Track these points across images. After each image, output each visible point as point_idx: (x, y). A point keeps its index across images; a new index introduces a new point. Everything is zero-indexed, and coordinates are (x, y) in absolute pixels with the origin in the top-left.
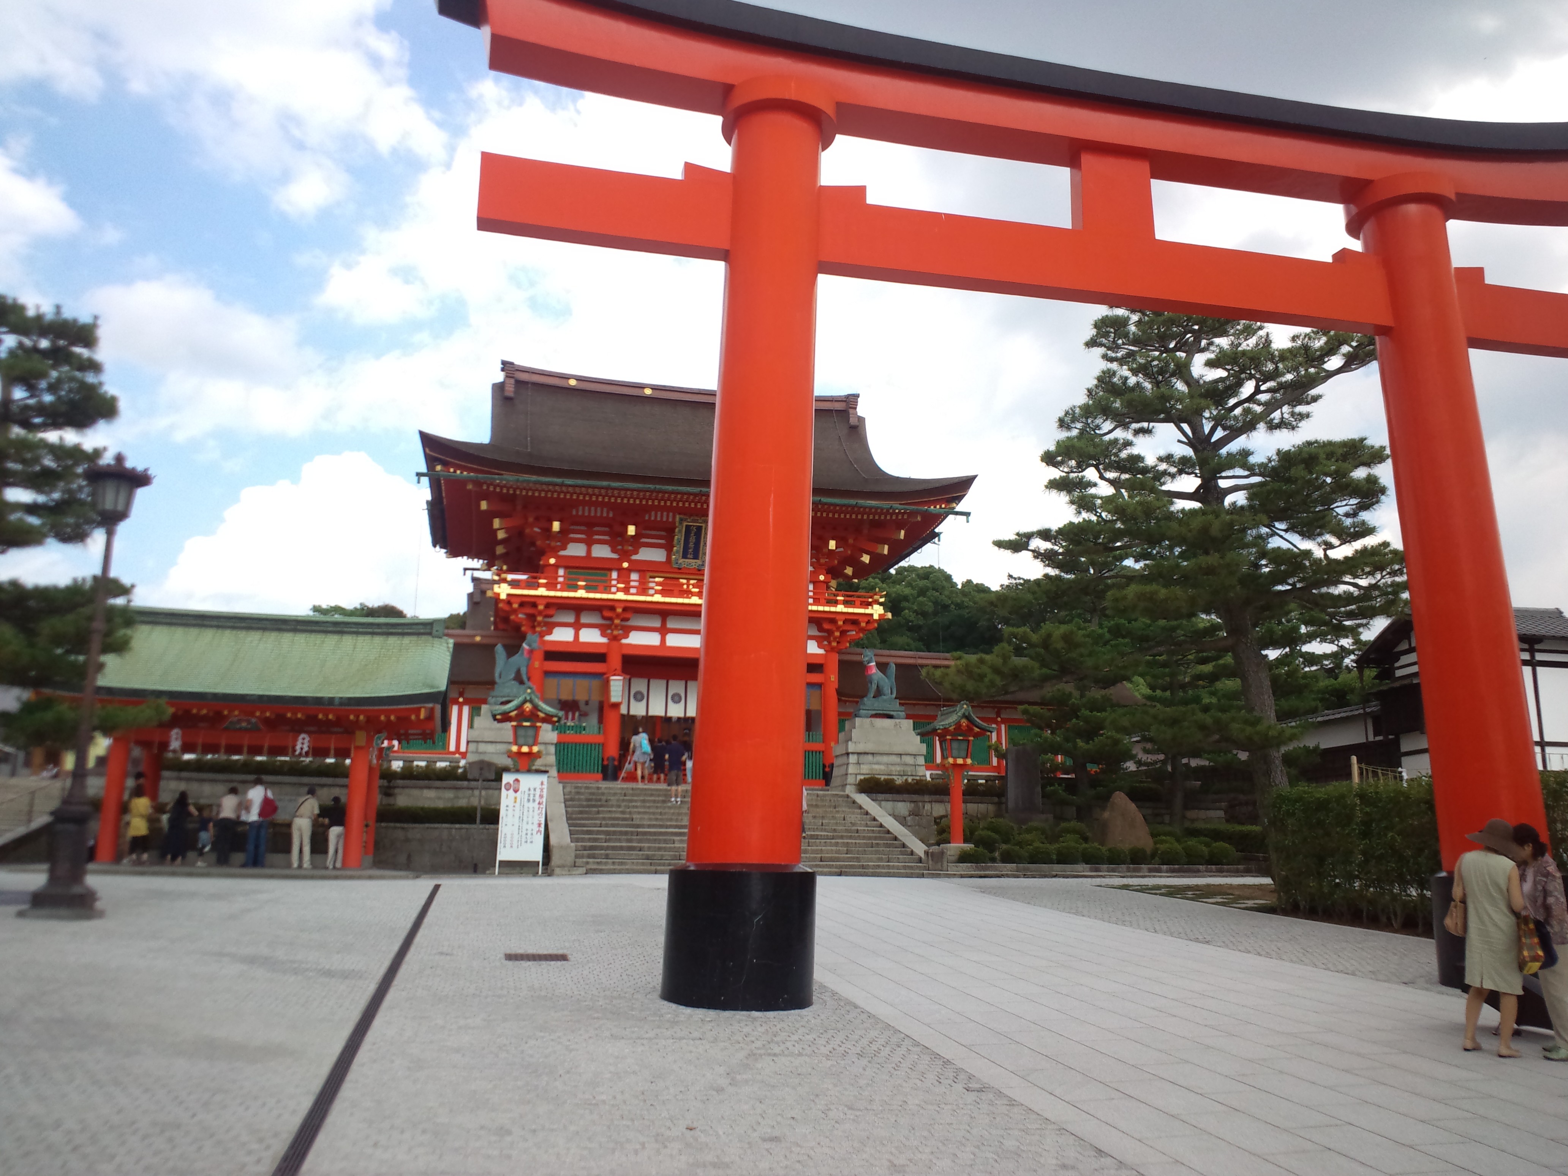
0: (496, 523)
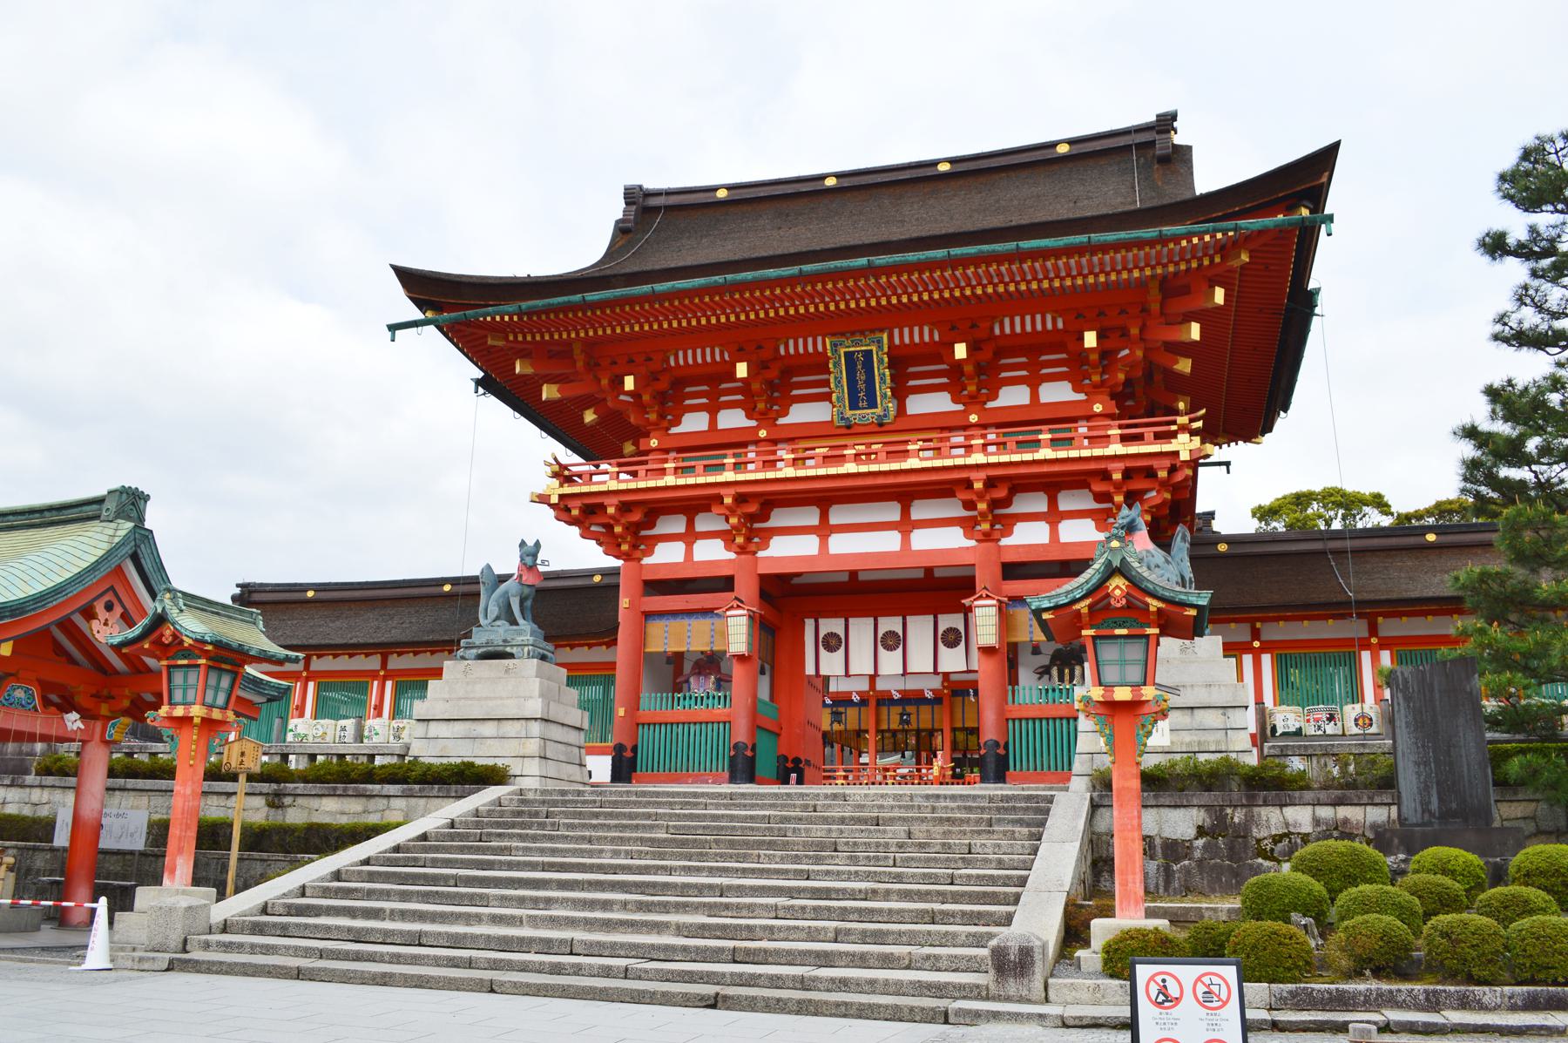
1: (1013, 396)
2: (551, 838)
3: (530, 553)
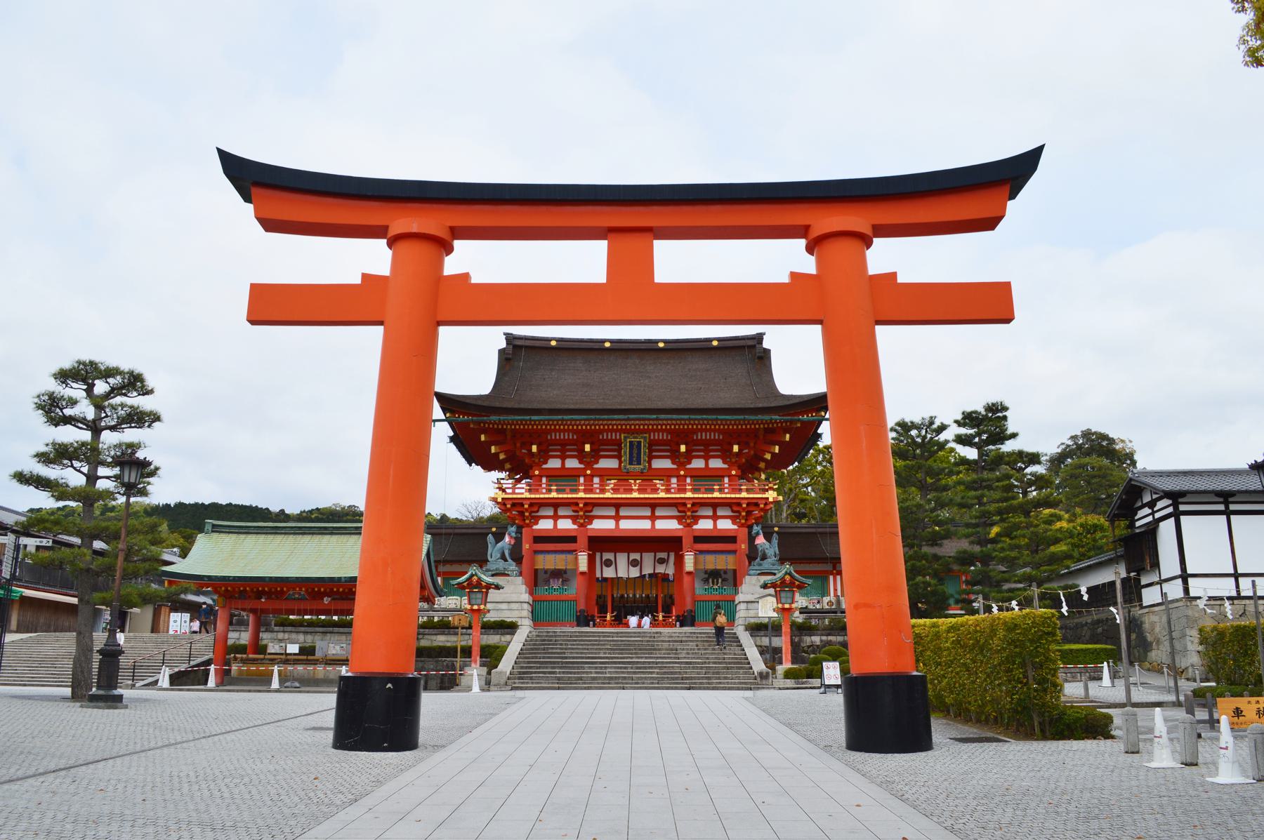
0: (493, 449)
1: (698, 464)
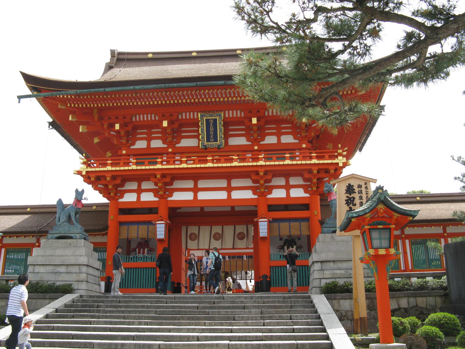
1: (271, 140)
2: (106, 317)
3: (79, 194)
